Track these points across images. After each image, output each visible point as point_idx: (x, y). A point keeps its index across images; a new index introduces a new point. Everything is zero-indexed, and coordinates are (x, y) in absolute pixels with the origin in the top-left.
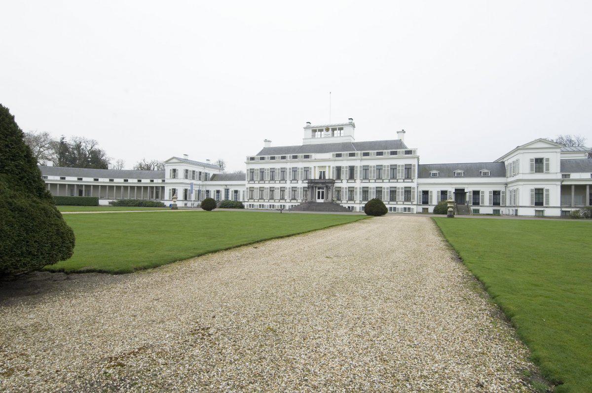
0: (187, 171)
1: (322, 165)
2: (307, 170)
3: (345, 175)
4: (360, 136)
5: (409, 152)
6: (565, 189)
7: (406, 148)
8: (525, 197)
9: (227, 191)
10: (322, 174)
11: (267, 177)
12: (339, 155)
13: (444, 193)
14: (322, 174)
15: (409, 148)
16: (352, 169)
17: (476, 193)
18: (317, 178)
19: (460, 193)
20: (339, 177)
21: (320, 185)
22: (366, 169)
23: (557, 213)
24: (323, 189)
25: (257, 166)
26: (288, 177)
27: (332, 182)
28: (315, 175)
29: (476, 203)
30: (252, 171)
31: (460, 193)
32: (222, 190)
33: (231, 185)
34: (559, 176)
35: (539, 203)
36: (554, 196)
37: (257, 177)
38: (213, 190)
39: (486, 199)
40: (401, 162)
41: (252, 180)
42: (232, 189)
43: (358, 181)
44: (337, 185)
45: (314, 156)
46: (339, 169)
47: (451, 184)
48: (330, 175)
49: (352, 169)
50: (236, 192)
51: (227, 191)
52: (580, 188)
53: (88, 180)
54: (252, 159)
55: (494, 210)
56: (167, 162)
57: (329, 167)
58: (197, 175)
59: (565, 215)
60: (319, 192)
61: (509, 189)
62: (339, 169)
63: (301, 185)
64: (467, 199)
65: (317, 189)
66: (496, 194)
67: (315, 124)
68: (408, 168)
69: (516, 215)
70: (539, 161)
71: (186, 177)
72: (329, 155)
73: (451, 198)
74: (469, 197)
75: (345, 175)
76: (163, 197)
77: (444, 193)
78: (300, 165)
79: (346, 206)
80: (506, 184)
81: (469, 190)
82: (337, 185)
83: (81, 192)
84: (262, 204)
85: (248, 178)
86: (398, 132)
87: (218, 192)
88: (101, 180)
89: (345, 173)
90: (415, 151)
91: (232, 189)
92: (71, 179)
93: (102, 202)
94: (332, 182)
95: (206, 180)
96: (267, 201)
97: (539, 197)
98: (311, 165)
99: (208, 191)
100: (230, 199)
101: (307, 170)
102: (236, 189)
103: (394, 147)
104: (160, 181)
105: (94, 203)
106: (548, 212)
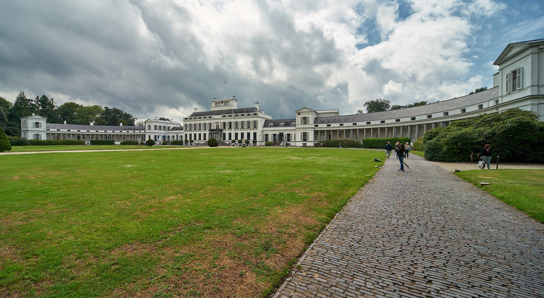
0: (156, 126)
1: (217, 121)
2: (210, 124)
3: (227, 127)
6: (316, 132)
8: (299, 138)
9: (177, 136)
10: (218, 126)
11: (239, 126)
12: (224, 116)
13: (275, 135)
14: (218, 126)
16: (230, 123)
18: (215, 128)
20: (224, 128)
22: (236, 123)
23: (312, 144)
25: (188, 123)
27: (221, 130)
28: (214, 127)
29: (289, 140)
30: (186, 125)
31: (281, 135)
32: (175, 135)
34: (313, 126)
35: (305, 140)
37: (188, 129)
38: (171, 135)
41: (186, 130)
42: (179, 135)
43: (233, 130)
44: (224, 132)
45: (213, 117)
48: (221, 127)
49: (230, 123)
51: (177, 136)
52: (322, 132)
53: (110, 132)
54: (186, 119)
58: (162, 128)
59: (316, 145)
62: (224, 123)
64: (284, 138)
70: (305, 118)
71: (156, 129)
72: (219, 116)
74: (285, 138)
75: (227, 127)
78: (207, 122)
81: (285, 133)
82: (224, 132)
83: (97, 138)
85: (184, 129)
87: (173, 136)
88: (116, 132)
91: (179, 135)
92: (101, 132)
93: (116, 143)
94: (221, 130)
95: (169, 130)
97: (305, 137)
98: (211, 122)
99: (169, 136)
101: (210, 124)
104: (143, 131)
105: (111, 143)
106: (308, 144)
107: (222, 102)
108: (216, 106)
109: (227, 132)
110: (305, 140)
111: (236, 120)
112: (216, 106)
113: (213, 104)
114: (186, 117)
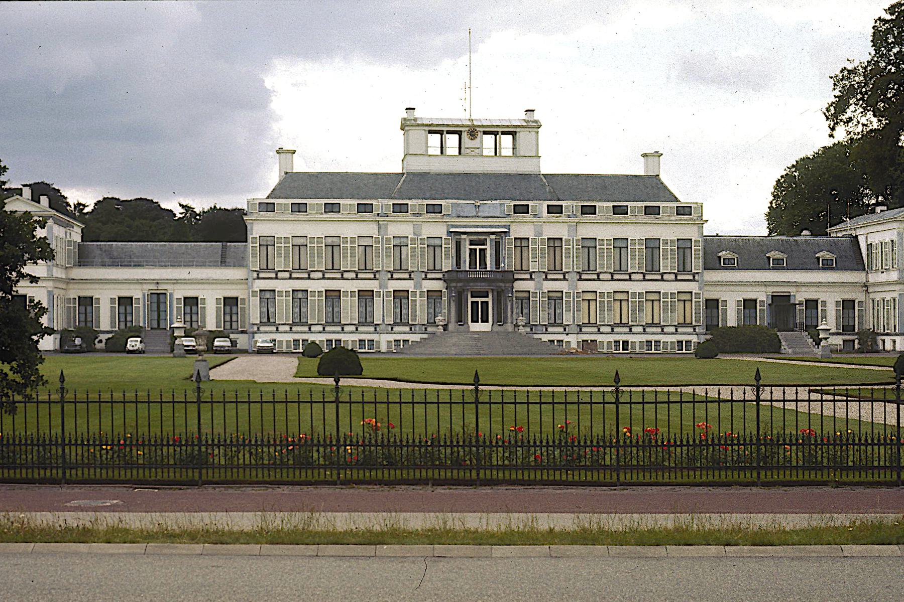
4: (556, 157)
5: (684, 211)
7: (676, 200)
15: (685, 198)
17: (812, 304)
21: (479, 287)
33: (176, 282)
40: (668, 232)
47: (765, 284)
50: (191, 302)
55: (844, 341)
61: (872, 296)
65: (469, 296)
66: (848, 305)
67: (424, 114)
68: (684, 246)
69: (894, 350)
80: (866, 286)
84: (367, 337)
86: (645, 155)
89: (539, 253)
90: (700, 207)
96: (320, 328)
102: (125, 293)
103: (643, 192)
111: (586, 231)
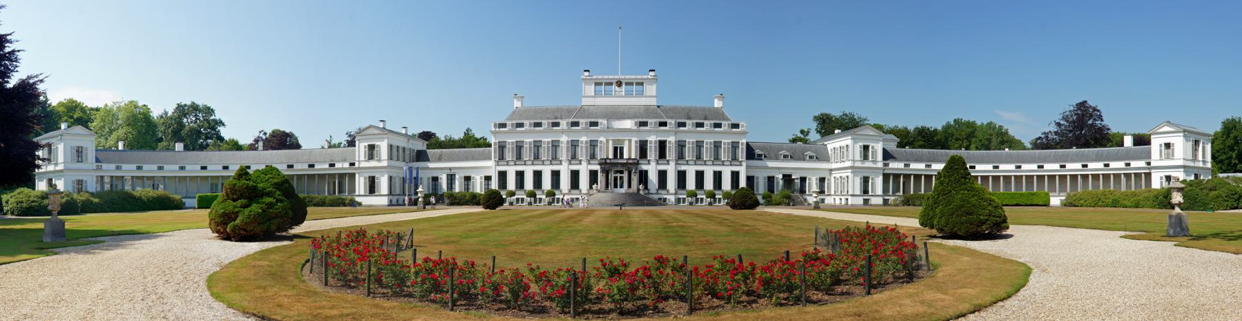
2: (593, 144)
3: (652, 154)
6: (886, 177)
10: (618, 151)
14: (618, 151)
19: (788, 179)
23: (879, 201)
24: (622, 172)
26: (564, 154)
29: (803, 191)
35: (865, 192)
36: (878, 184)
39: (813, 185)
46: (643, 148)
50: (468, 179)
54: (503, 125)
56: (360, 131)
57: (630, 141)
60: (616, 179)
63: (584, 170)
72: (628, 124)
73: (780, 182)
75: (652, 154)
76: (352, 190)
77: (771, 180)
79: (656, 197)
100: (457, 190)
107: (619, 84)
108: (597, 94)
109: (652, 170)
110: (865, 192)
112: (597, 94)
113: (590, 89)
114: (502, 121)
